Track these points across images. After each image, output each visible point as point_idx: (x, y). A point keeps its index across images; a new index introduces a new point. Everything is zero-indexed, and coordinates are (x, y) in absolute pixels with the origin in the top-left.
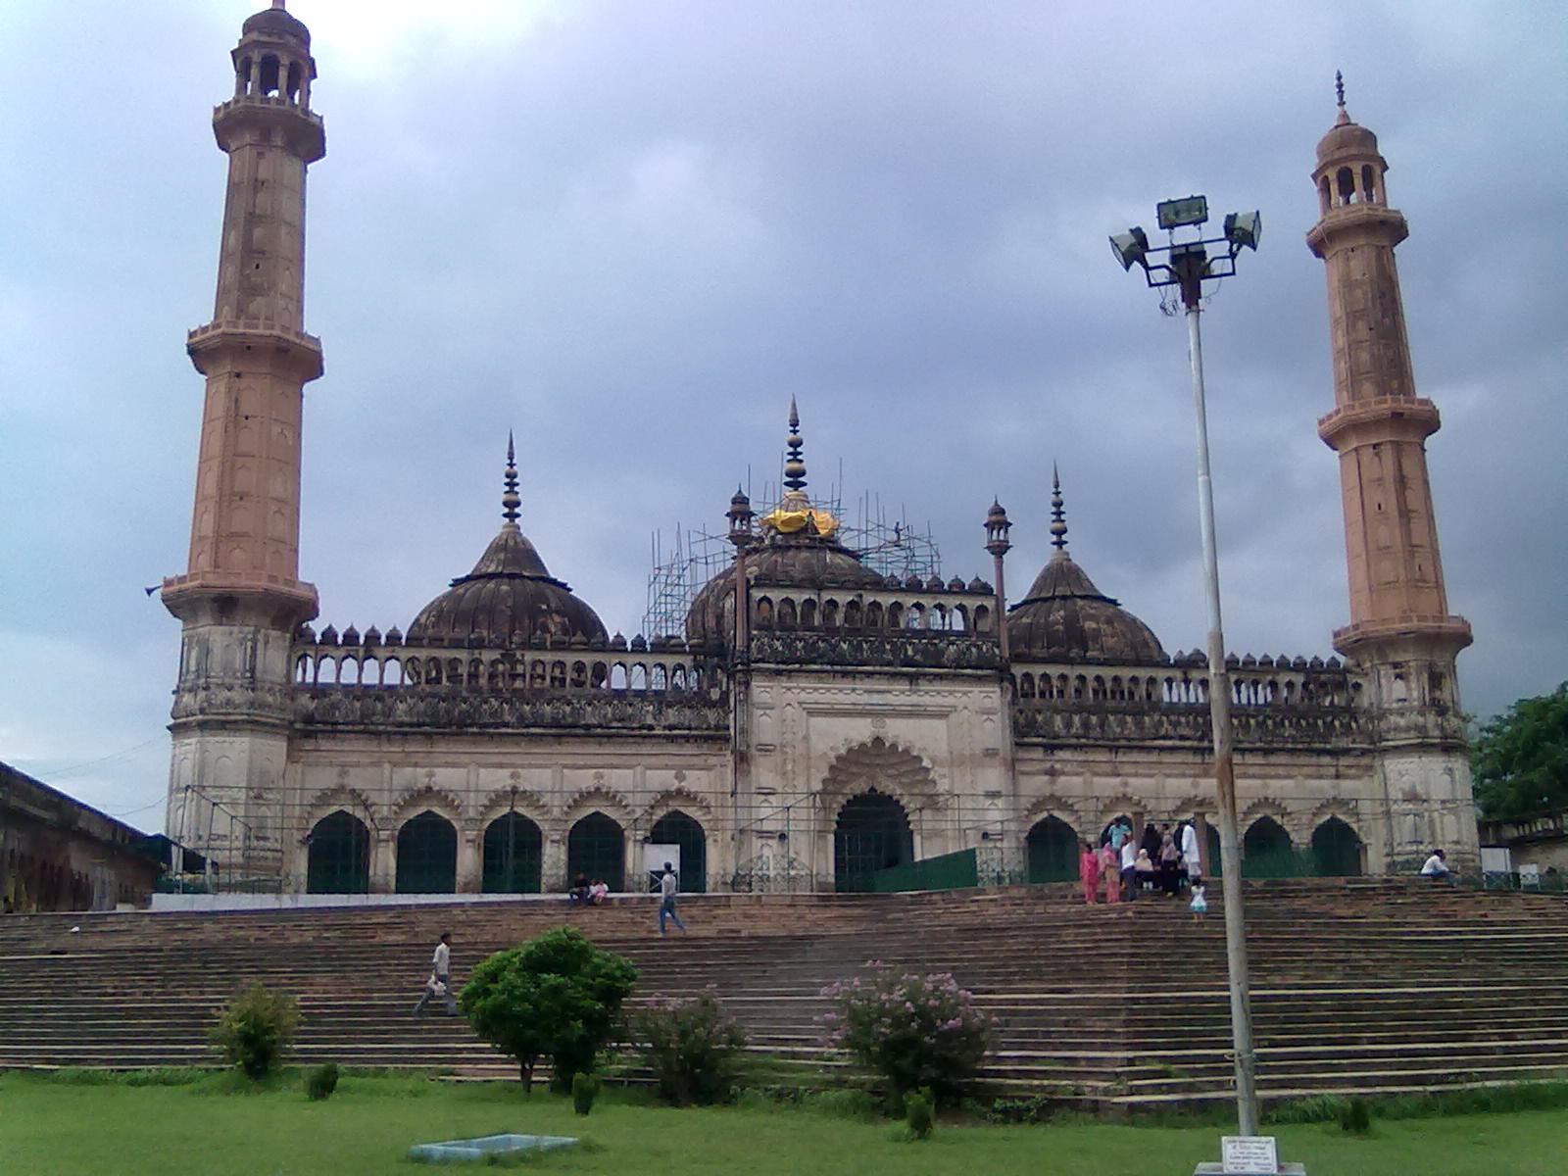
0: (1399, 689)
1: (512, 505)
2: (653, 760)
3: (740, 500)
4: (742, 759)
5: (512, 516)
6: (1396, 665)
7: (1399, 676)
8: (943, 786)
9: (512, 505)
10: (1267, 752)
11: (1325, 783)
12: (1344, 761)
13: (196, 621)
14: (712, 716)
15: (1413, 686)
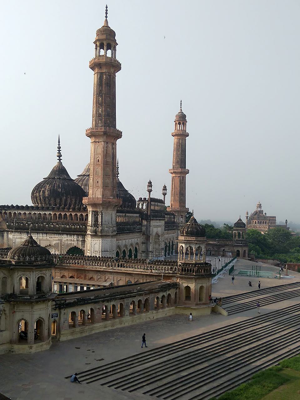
0: (181, 219)
1: (60, 156)
2: (136, 237)
3: (150, 183)
4: (148, 238)
5: (60, 160)
6: (182, 215)
7: (182, 217)
8: (160, 240)
9: (60, 156)
10: (171, 230)
11: (173, 234)
12: (175, 231)
13: (108, 209)
14: (140, 226)
15: (183, 219)
